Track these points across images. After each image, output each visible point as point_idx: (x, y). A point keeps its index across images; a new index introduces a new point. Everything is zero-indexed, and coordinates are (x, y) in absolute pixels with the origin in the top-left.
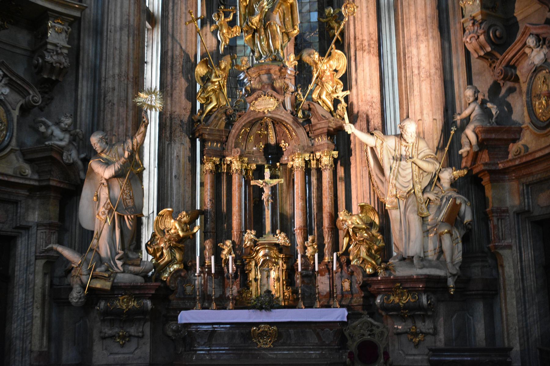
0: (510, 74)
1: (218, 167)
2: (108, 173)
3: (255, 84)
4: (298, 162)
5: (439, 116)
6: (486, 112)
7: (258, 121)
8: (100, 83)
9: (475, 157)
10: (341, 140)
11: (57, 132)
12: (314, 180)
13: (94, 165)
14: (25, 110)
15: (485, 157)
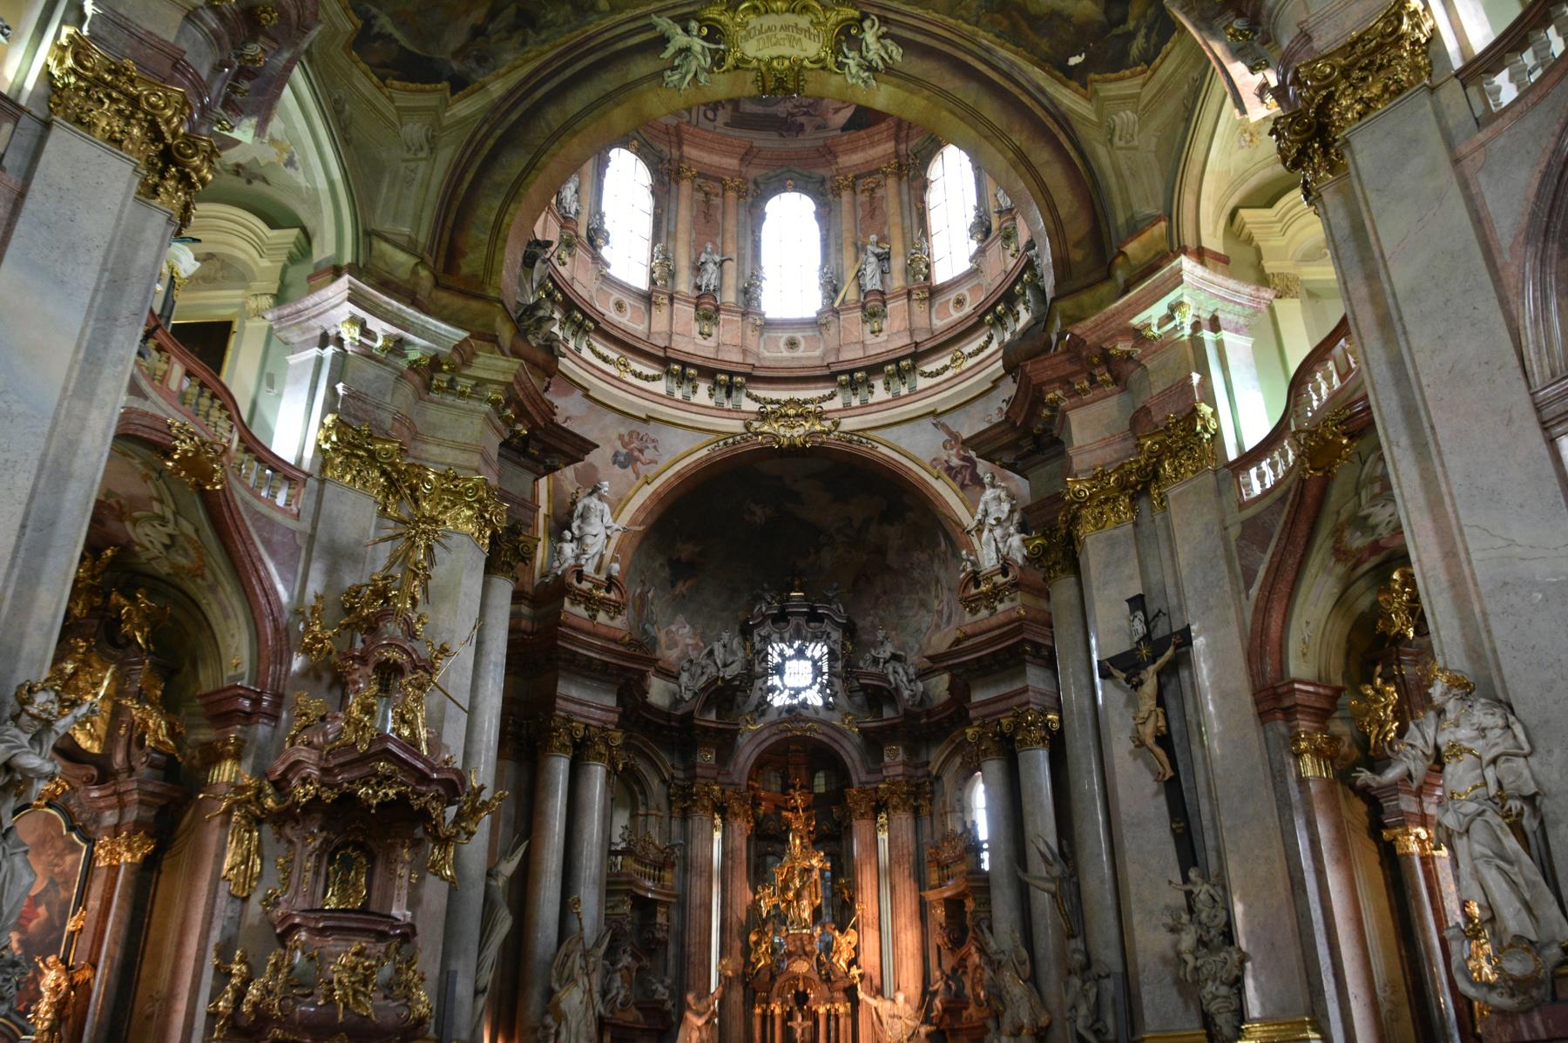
0: (962, 963)
1: (764, 1011)
2: (700, 1022)
3: (792, 948)
4: (822, 1010)
5: (919, 985)
6: (948, 987)
7: (796, 977)
8: (683, 946)
9: (941, 1019)
10: (851, 994)
11: (660, 988)
12: (832, 1023)
13: (689, 1015)
14: (638, 970)
15: (947, 1020)
